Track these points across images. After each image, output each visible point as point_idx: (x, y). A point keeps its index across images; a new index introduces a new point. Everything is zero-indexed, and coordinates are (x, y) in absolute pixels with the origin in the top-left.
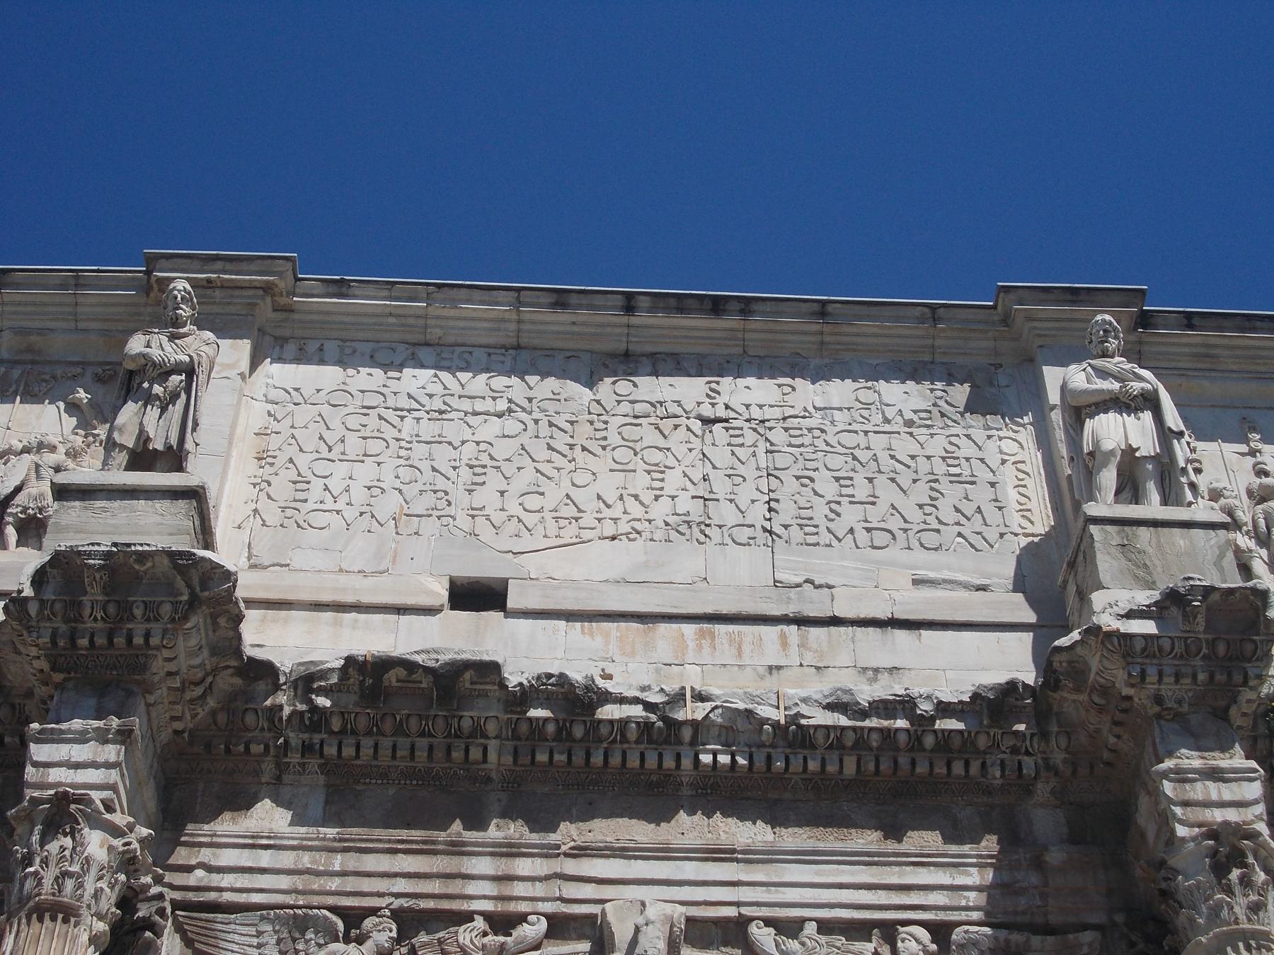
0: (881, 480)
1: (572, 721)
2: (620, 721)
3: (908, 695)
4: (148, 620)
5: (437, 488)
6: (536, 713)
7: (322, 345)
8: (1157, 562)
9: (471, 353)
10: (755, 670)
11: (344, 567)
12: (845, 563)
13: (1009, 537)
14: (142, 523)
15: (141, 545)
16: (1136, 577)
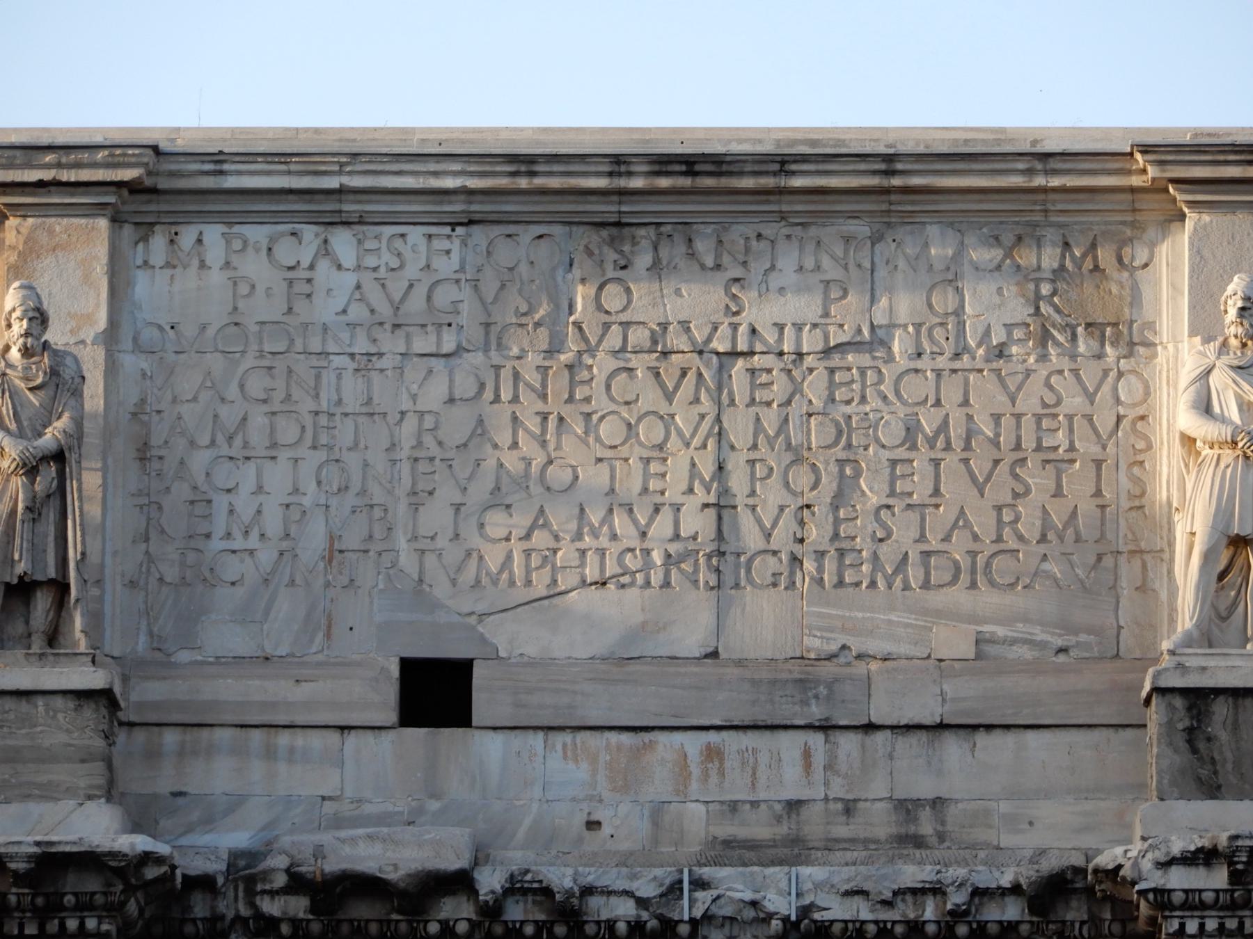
0: (951, 461)
1: (553, 923)
2: (608, 921)
3: (939, 882)
4: (82, 910)
5: (374, 502)
6: (515, 912)
7: (201, 233)
8: (1229, 755)
9: (403, 235)
10: (771, 808)
11: (269, 650)
12: (893, 617)
13: (1108, 561)
14: (47, 743)
15: (67, 843)
16: (1199, 780)
